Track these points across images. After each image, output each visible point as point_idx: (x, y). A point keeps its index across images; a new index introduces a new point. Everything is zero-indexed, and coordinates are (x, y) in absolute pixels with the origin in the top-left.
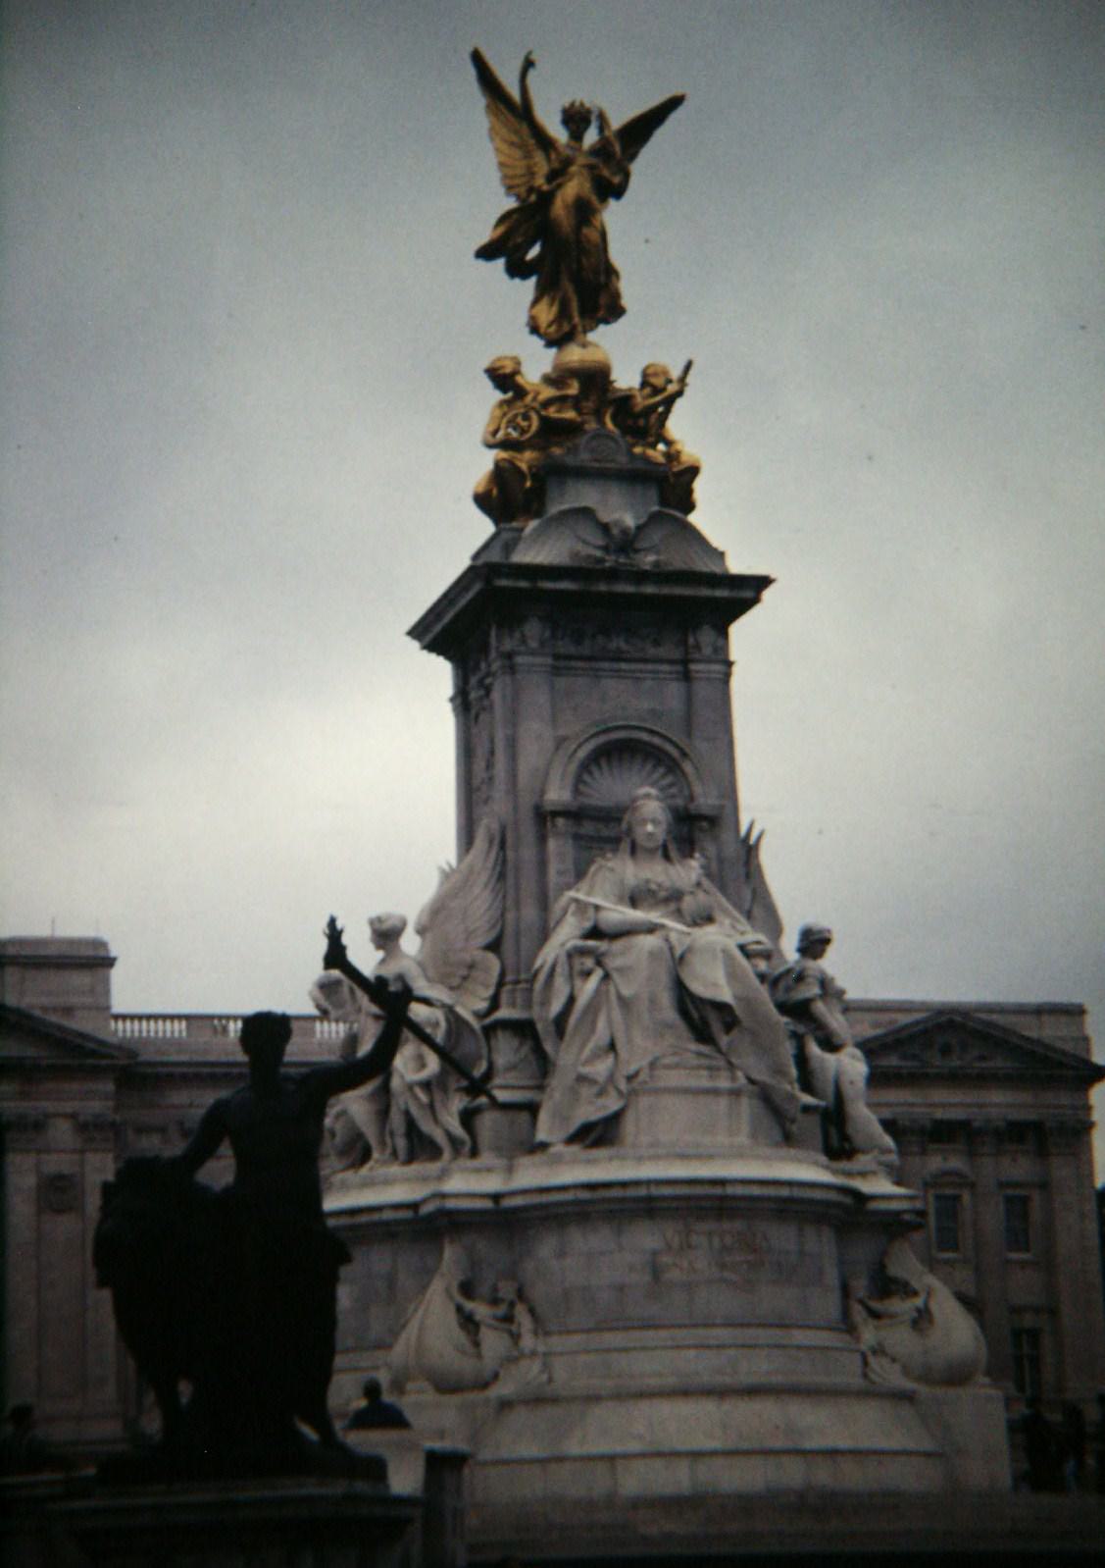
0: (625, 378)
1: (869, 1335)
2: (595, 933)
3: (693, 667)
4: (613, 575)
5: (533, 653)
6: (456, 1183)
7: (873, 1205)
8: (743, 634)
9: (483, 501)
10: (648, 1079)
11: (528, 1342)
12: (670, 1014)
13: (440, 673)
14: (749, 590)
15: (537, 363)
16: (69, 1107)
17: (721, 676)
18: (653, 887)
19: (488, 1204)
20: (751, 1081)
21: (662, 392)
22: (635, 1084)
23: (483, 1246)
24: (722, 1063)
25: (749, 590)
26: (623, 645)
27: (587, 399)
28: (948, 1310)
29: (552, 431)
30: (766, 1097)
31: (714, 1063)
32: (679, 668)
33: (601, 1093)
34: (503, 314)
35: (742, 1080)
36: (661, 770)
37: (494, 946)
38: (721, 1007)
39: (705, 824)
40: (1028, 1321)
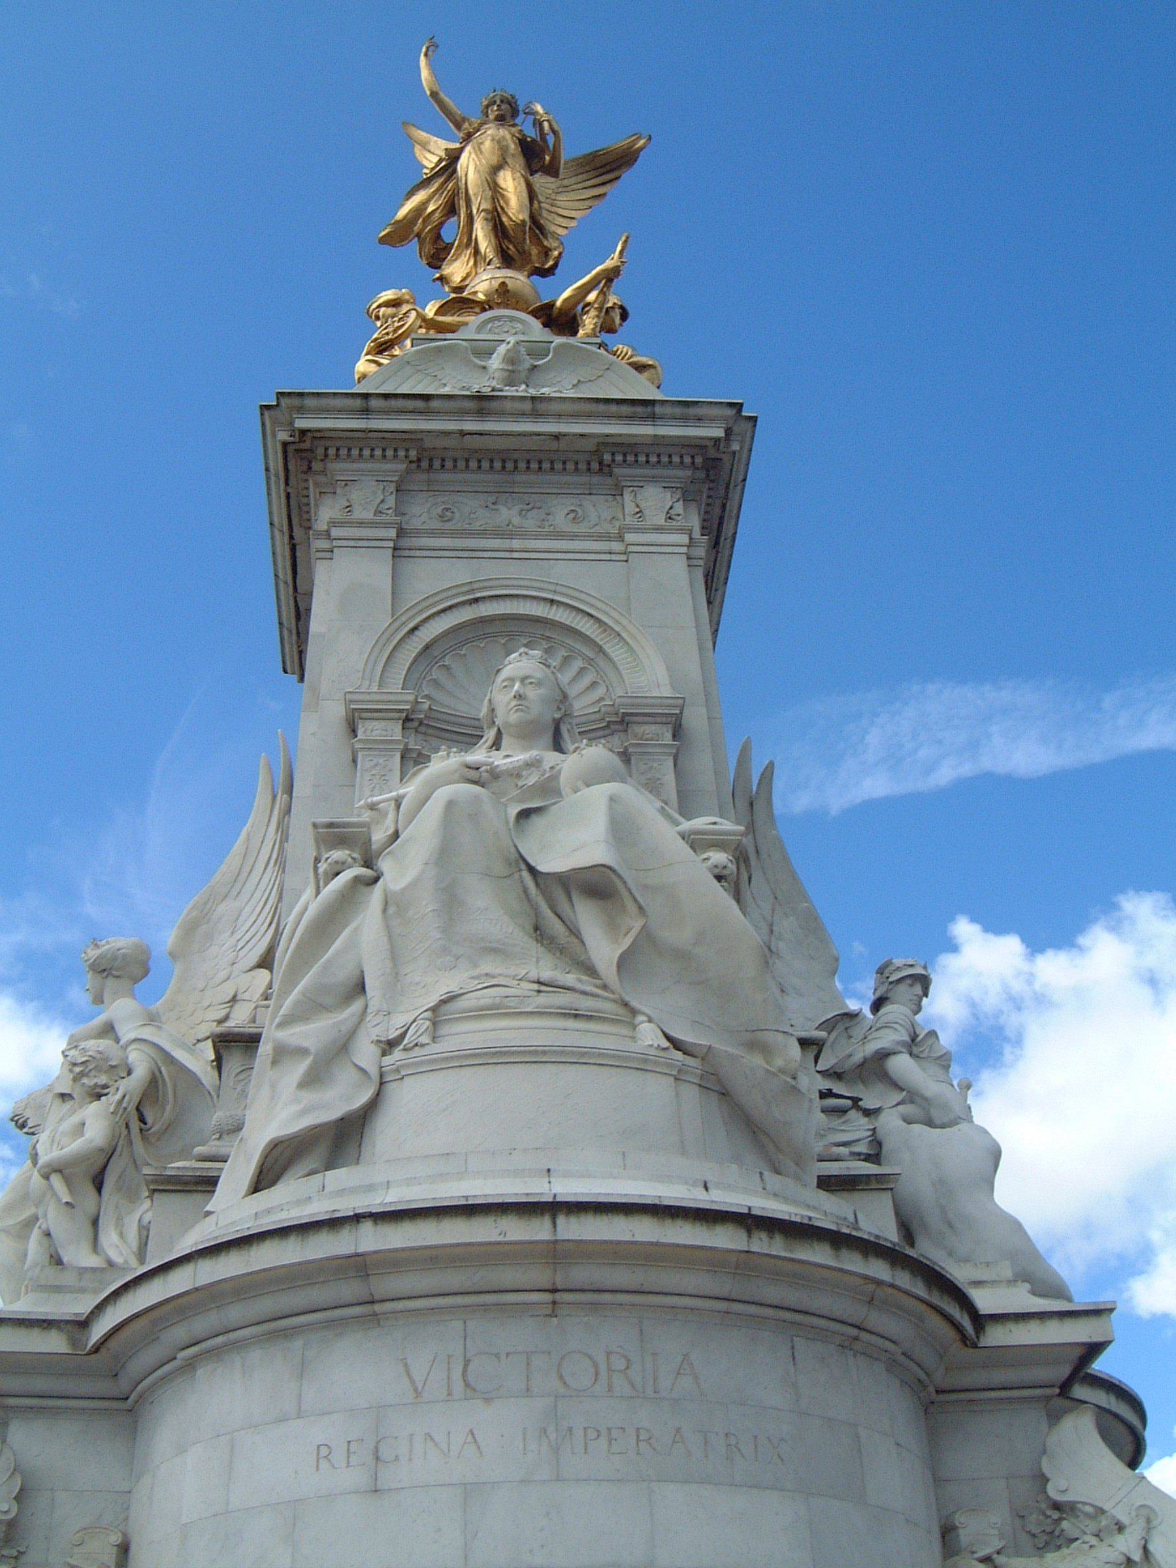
3: (629, 537)
4: (482, 403)
5: (361, 524)
10: (425, 1039)
17: (684, 550)
20: (676, 1044)
22: (397, 1054)
24: (609, 1007)
26: (516, 521)
31: (585, 1004)
32: (616, 546)
33: (313, 1079)
35: (648, 1036)
36: (578, 664)
38: (597, 886)
39: (650, 729)
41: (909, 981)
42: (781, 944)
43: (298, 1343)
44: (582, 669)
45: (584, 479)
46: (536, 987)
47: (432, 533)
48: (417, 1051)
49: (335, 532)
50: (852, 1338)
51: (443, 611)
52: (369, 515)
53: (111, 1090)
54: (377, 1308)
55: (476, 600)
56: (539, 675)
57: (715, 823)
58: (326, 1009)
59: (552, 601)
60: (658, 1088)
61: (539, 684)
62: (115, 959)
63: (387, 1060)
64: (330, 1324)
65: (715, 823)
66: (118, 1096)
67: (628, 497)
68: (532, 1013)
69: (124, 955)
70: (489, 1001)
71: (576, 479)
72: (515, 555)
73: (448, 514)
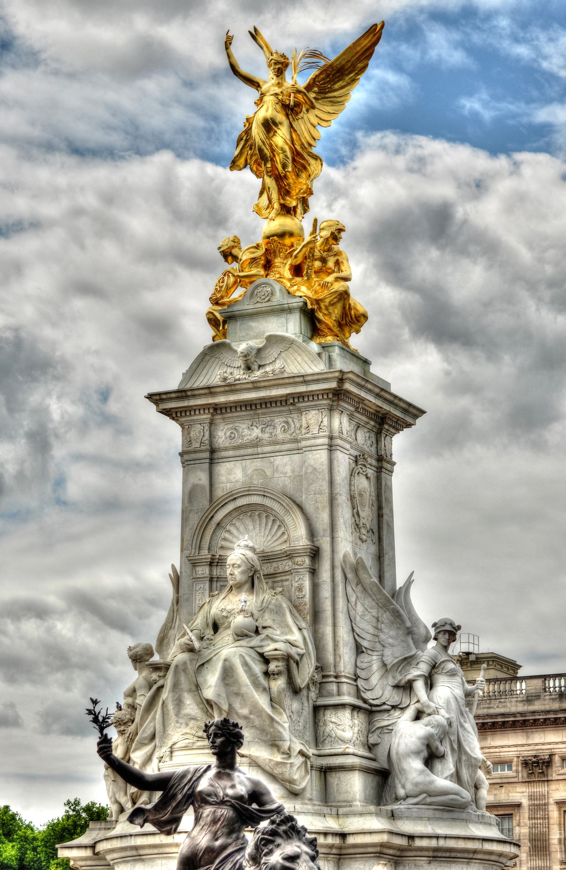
7: (351, 840)
18: (224, 614)
27: (275, 256)
39: (299, 560)
41: (442, 633)
42: (383, 626)
43: (129, 864)
44: (279, 526)
45: (287, 408)
46: (196, 739)
47: (226, 449)
48: (165, 763)
49: (186, 457)
51: (222, 506)
52: (198, 445)
53: (126, 731)
54: (141, 857)
55: (235, 499)
56: (239, 562)
57: (276, 650)
58: (145, 744)
59: (264, 496)
61: (239, 566)
62: (136, 656)
63: (161, 764)
64: (135, 860)
65: (276, 650)
66: (128, 735)
67: (304, 419)
68: (196, 749)
69: (140, 655)
70: (184, 745)
71: (283, 408)
72: (260, 456)
73: (232, 435)
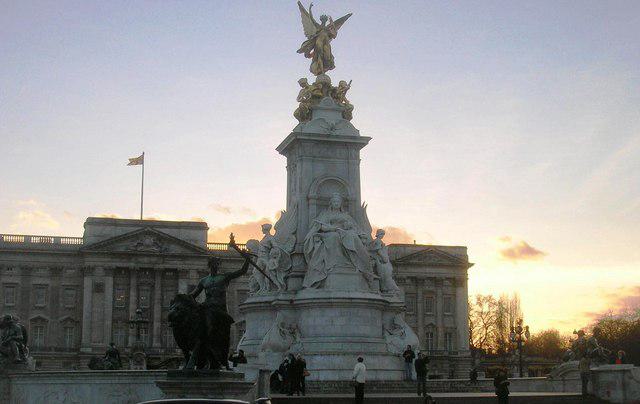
0: (335, 84)
1: (389, 339)
2: (321, 231)
6: (281, 297)
8: (363, 152)
9: (296, 115)
11: (298, 339)
12: (340, 253)
13: (283, 160)
14: (365, 141)
15: (312, 79)
16: (196, 267)
19: (288, 303)
21: (344, 87)
23: (286, 313)
25: (365, 141)
28: (408, 330)
29: (314, 97)
30: (364, 276)
34: (303, 68)
37: (295, 233)
40: (449, 330)
50: (377, 308)
60: (358, 278)
